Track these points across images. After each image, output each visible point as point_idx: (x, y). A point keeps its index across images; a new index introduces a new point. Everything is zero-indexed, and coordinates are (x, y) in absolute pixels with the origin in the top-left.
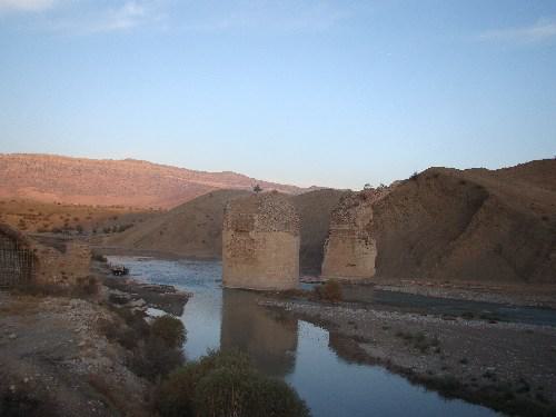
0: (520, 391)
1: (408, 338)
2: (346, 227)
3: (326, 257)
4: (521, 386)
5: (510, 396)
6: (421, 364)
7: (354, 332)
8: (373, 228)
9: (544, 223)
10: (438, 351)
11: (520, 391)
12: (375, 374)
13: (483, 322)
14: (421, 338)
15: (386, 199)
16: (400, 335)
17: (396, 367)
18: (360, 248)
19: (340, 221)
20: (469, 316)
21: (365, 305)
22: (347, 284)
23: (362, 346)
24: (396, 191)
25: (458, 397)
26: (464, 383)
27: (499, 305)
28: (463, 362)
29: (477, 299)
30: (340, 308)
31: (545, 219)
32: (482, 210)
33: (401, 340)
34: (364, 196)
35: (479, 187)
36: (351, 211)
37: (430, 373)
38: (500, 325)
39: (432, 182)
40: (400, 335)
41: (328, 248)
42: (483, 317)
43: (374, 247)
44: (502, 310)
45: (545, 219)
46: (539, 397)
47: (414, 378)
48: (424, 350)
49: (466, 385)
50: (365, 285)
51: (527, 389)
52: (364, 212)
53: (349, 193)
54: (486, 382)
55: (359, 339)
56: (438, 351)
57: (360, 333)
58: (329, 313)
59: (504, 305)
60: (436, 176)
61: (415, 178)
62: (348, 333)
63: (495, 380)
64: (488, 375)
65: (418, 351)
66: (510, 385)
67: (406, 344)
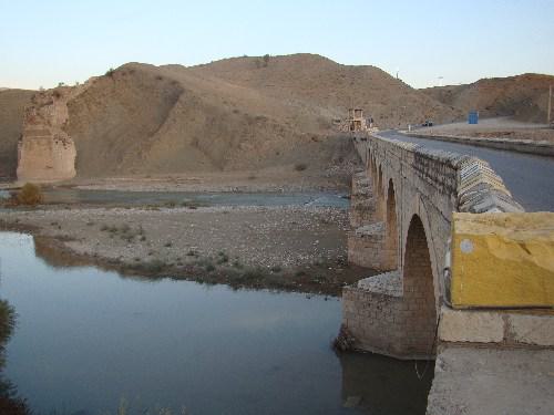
0: (219, 263)
1: (114, 230)
2: (40, 127)
3: (21, 162)
4: (221, 258)
5: (211, 268)
6: (128, 253)
7: (56, 232)
8: (70, 127)
9: (235, 115)
10: (144, 239)
11: (219, 263)
12: (90, 276)
13: (184, 209)
14: (126, 229)
15: (82, 95)
16: (105, 229)
17: (130, 267)
18: (57, 148)
19: (31, 120)
20: (172, 205)
21: (68, 206)
22: (46, 188)
23: (67, 244)
24: (92, 87)
25: (165, 277)
26: (168, 263)
27: (198, 193)
28: (169, 245)
29: (178, 190)
30: (40, 211)
31: (236, 112)
32: (178, 103)
33: (106, 234)
34: (57, 93)
35: (174, 83)
36: (45, 109)
37: (138, 260)
38: (199, 209)
39: (129, 77)
40: (105, 229)
41: (22, 151)
42: (185, 205)
43: (73, 146)
44: (200, 197)
45: (236, 112)
46: (236, 264)
47: (125, 270)
48: (130, 239)
49: (172, 265)
50: (67, 186)
51: (226, 260)
52: (59, 113)
53: (42, 93)
54: (188, 260)
55: (62, 239)
56: (144, 239)
57: (63, 233)
58: (31, 216)
59: (205, 193)
60: (132, 72)
61: (111, 74)
62: (53, 235)
63: (197, 257)
64: (191, 254)
65: (125, 242)
66: (211, 258)
67: (112, 237)
